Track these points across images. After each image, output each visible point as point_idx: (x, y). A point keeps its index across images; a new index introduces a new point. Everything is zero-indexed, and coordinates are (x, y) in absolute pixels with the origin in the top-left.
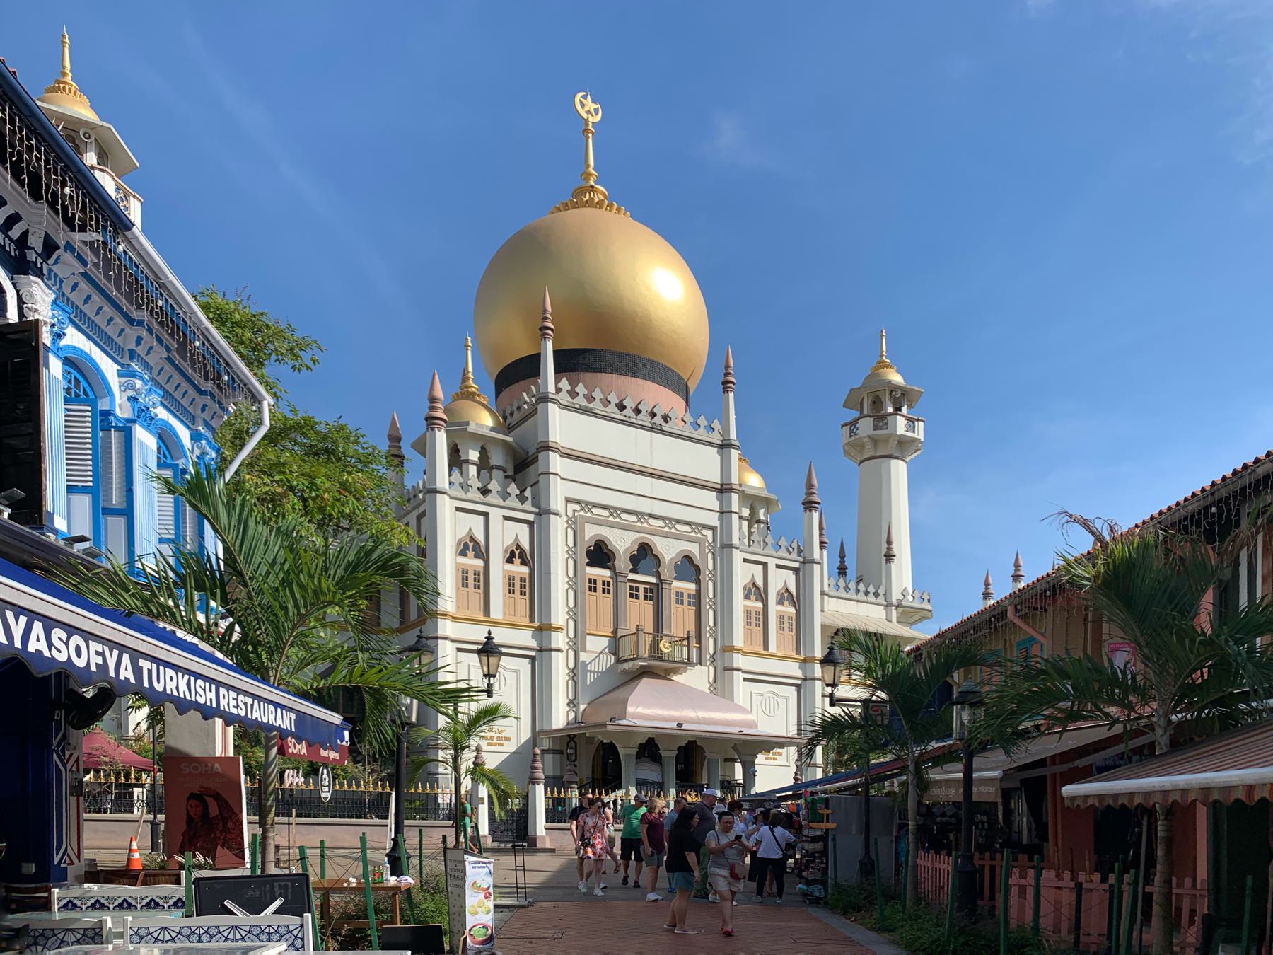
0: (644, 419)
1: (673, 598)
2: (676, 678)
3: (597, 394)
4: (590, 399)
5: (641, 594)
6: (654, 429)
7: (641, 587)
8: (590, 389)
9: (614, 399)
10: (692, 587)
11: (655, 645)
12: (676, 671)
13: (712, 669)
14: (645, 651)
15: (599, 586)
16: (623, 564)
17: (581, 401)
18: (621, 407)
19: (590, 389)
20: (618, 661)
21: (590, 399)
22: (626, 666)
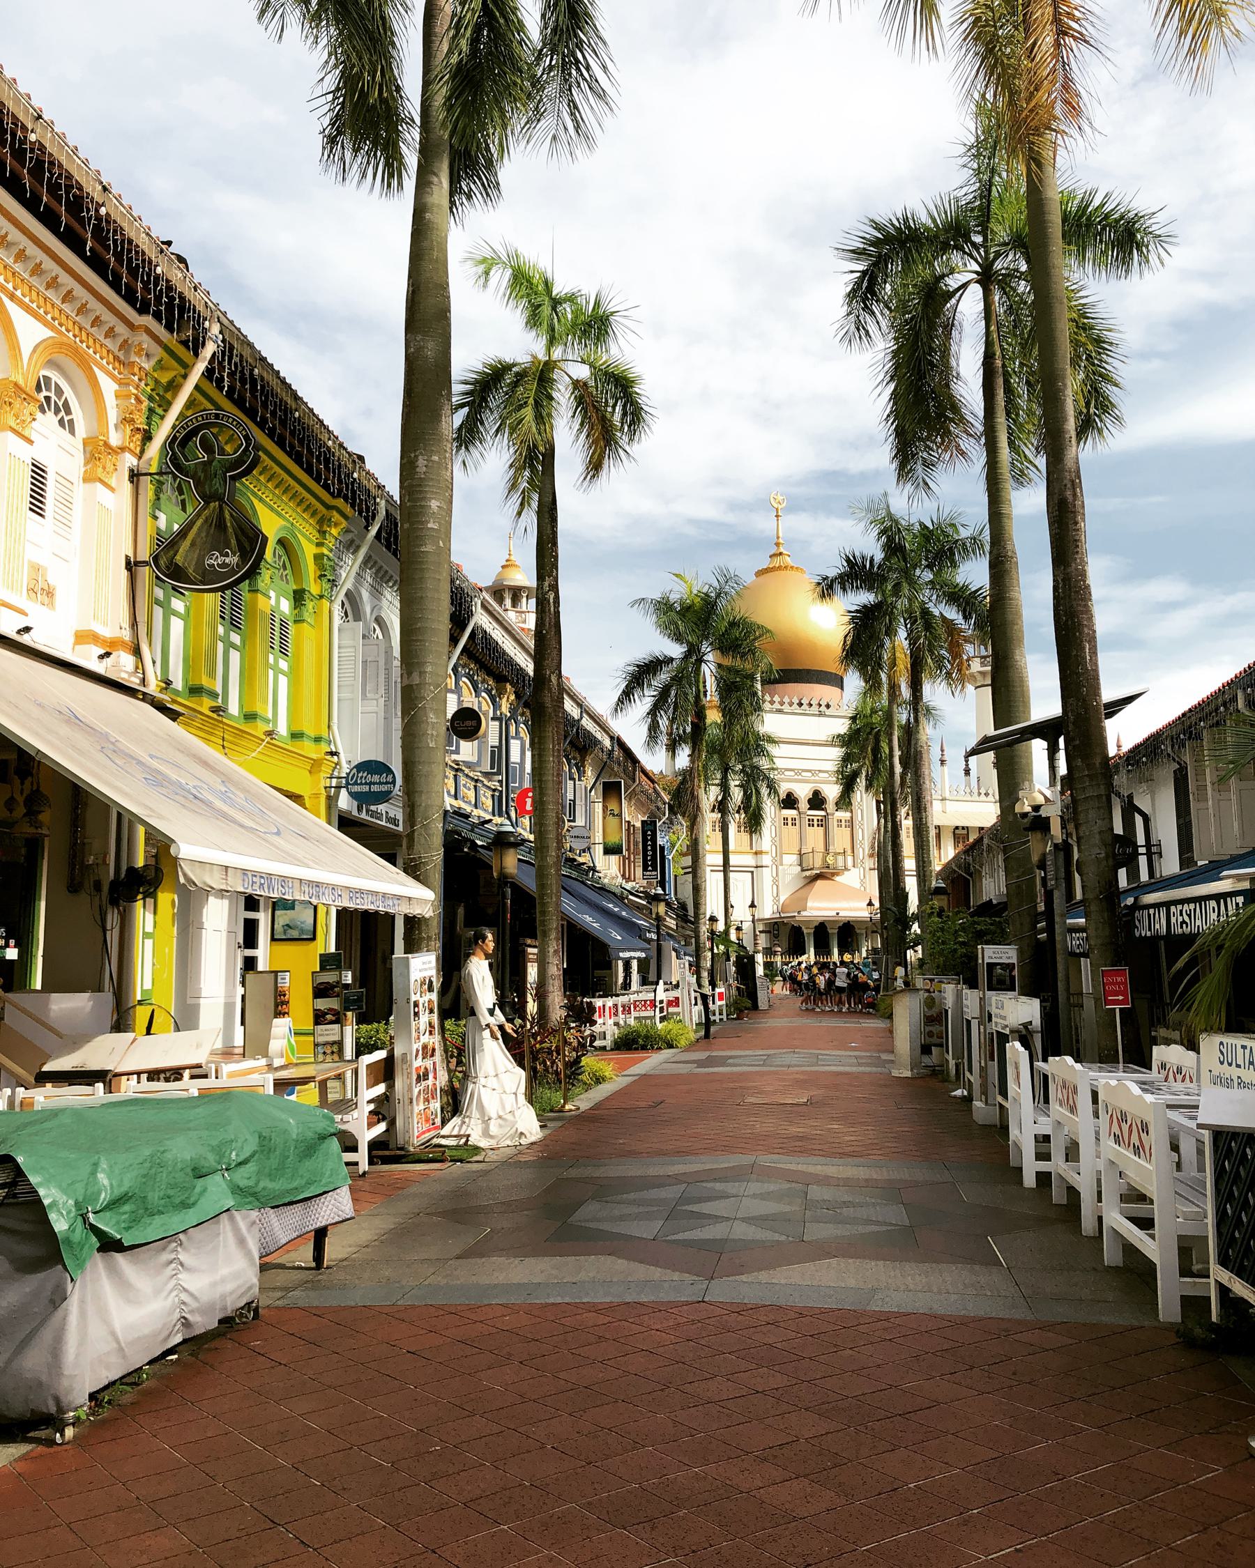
0: (815, 709)
1: (836, 823)
2: (837, 878)
3: (786, 700)
4: (782, 703)
5: (816, 823)
6: (821, 714)
7: (815, 818)
8: (782, 697)
9: (796, 701)
10: (848, 815)
11: (824, 860)
12: (837, 874)
13: (862, 869)
14: (818, 863)
15: (790, 822)
16: (803, 805)
17: (777, 706)
18: (800, 704)
19: (782, 697)
20: (803, 870)
21: (782, 703)
22: (808, 873)
